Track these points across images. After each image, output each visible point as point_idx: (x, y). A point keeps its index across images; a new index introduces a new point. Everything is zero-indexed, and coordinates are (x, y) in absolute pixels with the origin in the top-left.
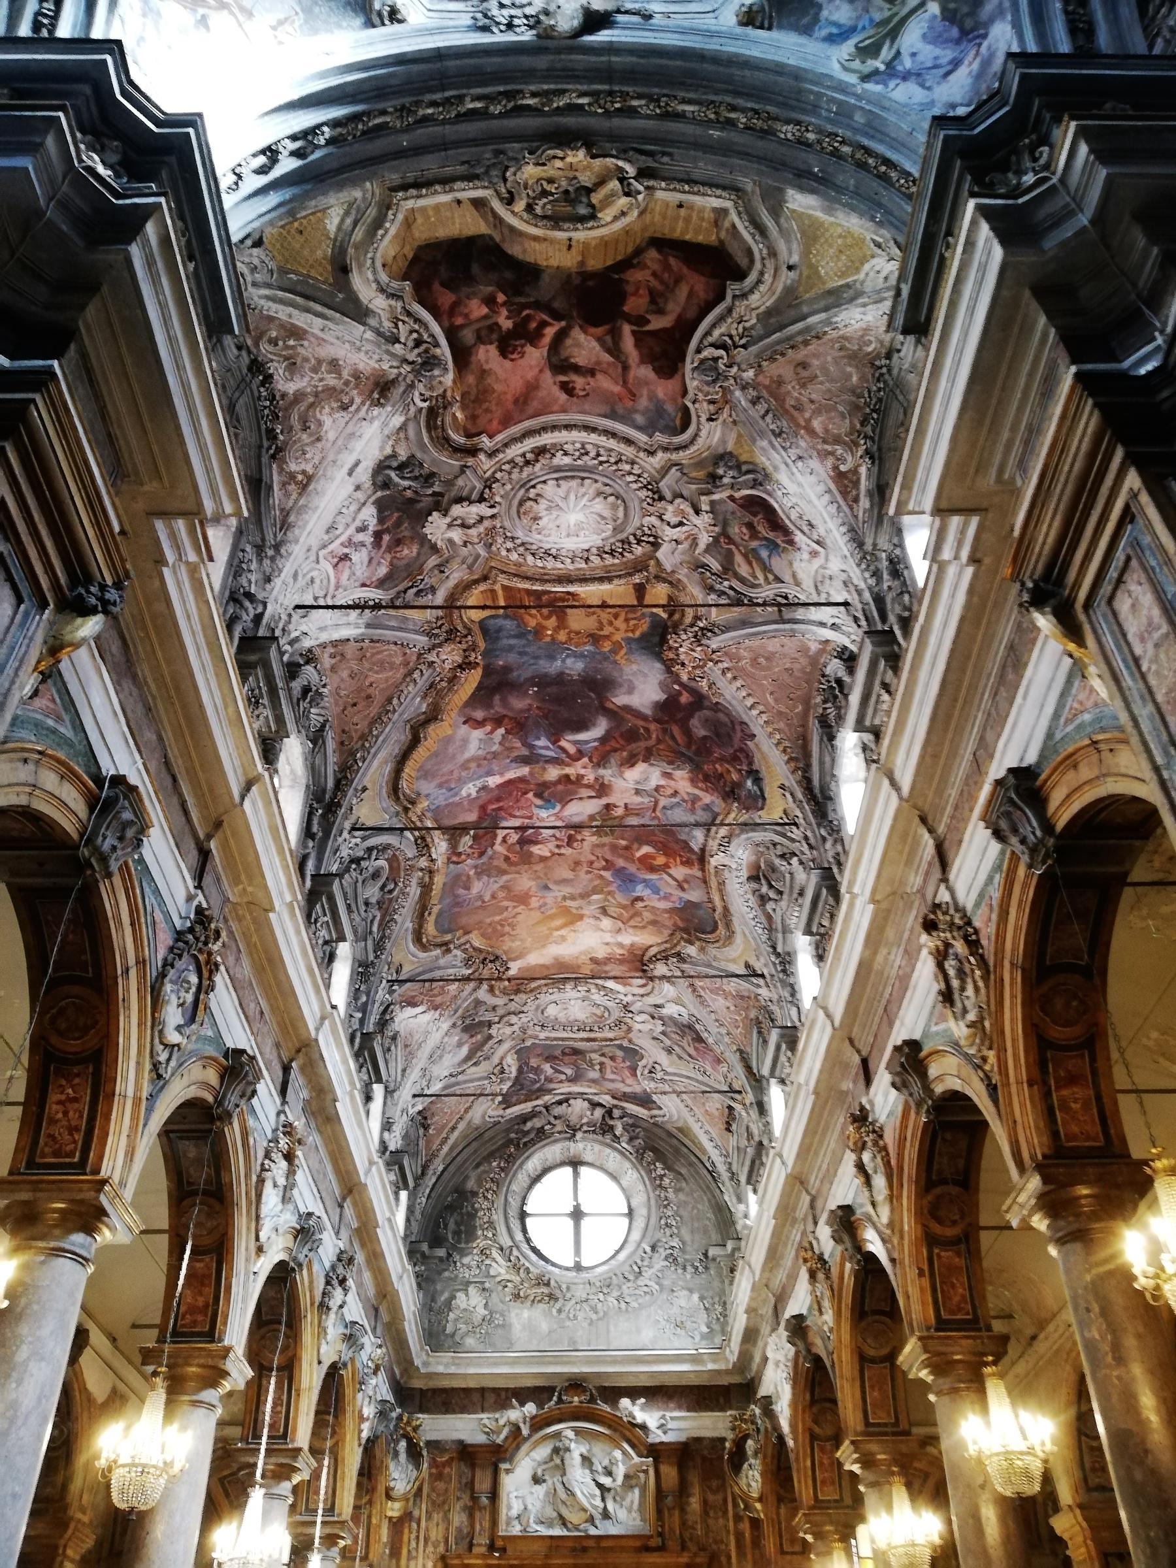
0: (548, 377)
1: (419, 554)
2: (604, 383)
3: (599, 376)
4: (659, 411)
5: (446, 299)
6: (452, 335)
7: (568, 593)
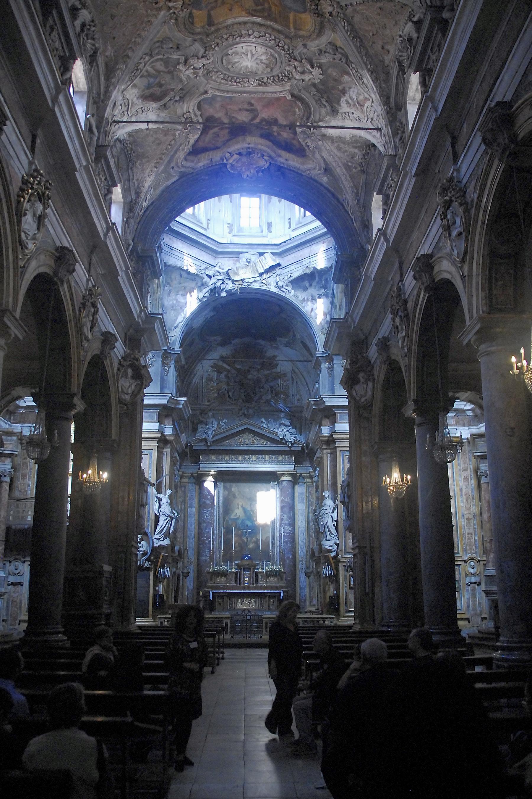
0: (259, 108)
1: (329, 67)
2: (236, 108)
3: (237, 109)
4: (210, 104)
5: (295, 142)
6: (295, 133)
7: (253, 15)
